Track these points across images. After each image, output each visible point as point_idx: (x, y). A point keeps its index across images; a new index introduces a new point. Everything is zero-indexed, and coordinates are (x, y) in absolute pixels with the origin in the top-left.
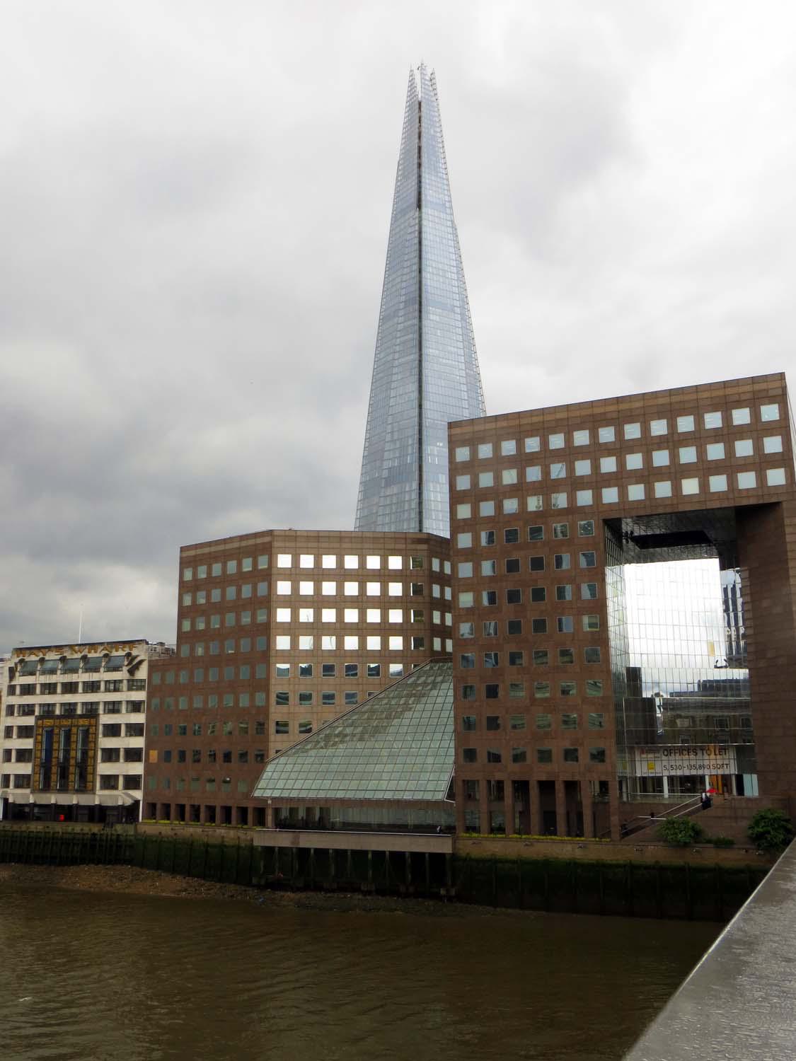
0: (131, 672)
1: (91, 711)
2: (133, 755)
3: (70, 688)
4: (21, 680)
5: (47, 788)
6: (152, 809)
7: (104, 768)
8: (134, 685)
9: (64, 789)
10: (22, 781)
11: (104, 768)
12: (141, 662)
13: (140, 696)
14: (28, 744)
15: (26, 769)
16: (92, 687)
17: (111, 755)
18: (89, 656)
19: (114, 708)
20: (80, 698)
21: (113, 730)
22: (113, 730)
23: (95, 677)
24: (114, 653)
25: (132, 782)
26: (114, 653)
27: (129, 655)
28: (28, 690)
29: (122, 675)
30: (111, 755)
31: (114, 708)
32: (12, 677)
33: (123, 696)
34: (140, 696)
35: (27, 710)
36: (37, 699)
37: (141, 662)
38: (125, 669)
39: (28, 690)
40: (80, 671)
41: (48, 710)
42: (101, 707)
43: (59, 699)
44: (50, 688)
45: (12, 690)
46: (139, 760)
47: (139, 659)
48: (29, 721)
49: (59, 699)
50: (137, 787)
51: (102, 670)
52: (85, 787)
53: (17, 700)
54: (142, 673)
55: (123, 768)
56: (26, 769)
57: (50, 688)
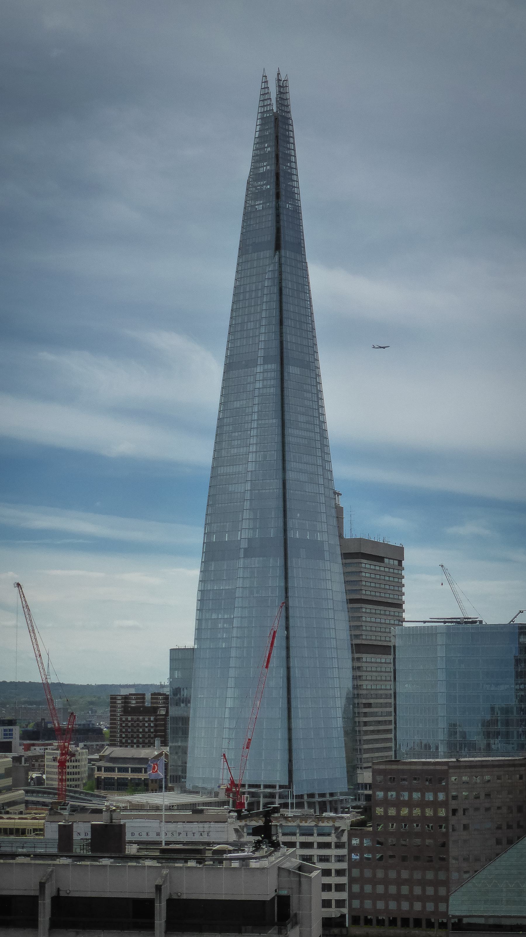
0: (338, 837)
6: (355, 920)
8: (339, 846)
12: (343, 831)
13: (344, 852)
18: (301, 824)
23: (309, 839)
24: (321, 824)
25: (340, 903)
26: (321, 824)
27: (334, 826)
32: (240, 836)
33: (332, 852)
34: (344, 852)
37: (343, 831)
38: (333, 835)
40: (298, 835)
42: (315, 859)
46: (344, 890)
47: (341, 829)
50: (344, 907)
51: (315, 835)
54: (345, 838)
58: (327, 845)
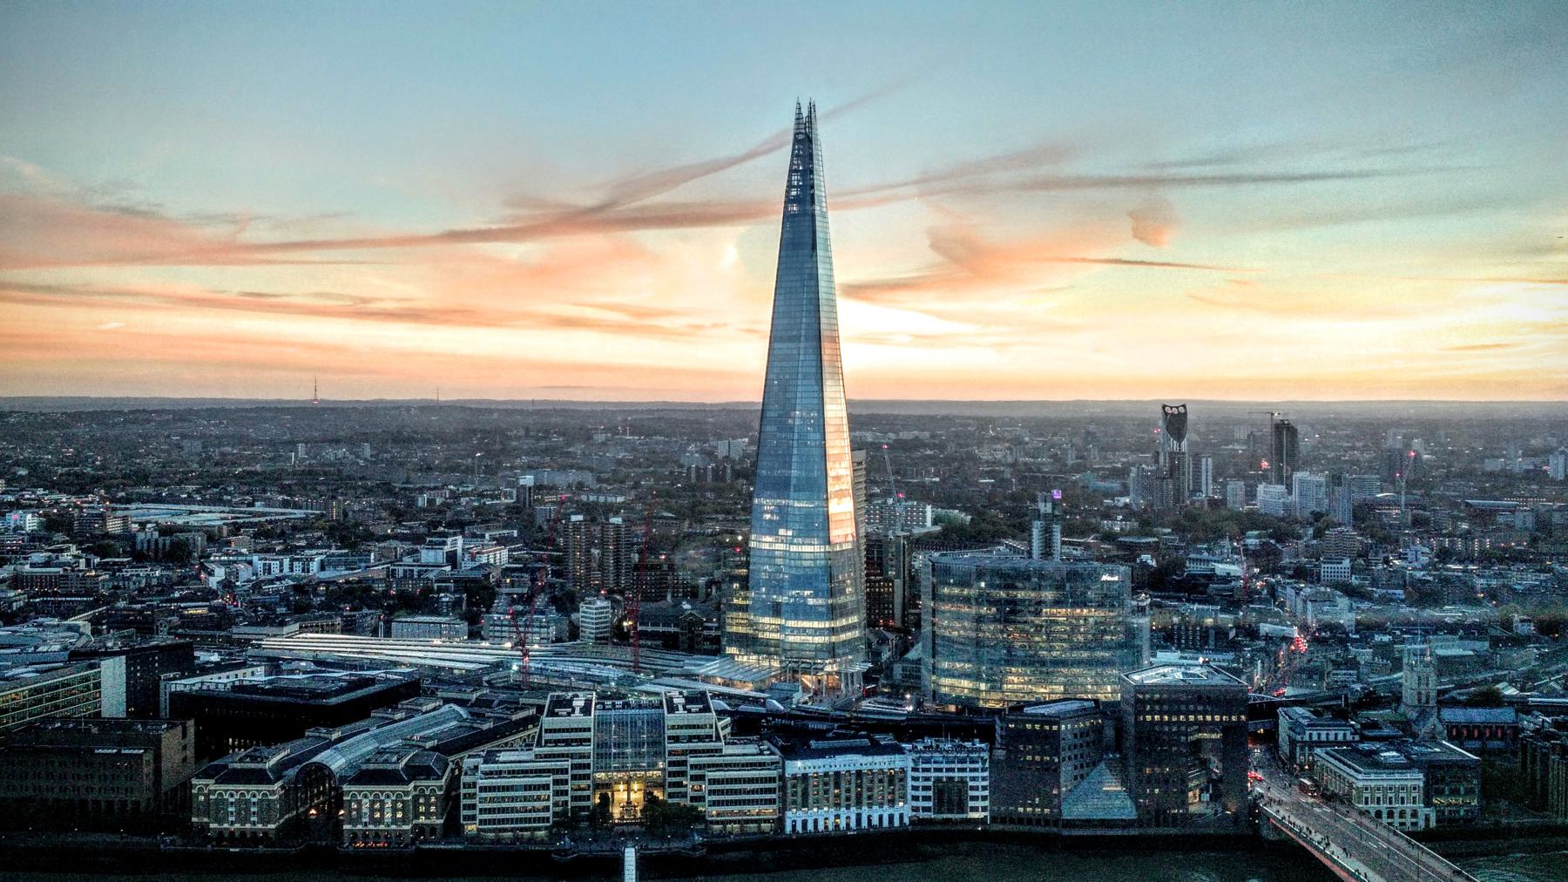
1: (963, 781)
2: (984, 798)
3: (952, 770)
4: (921, 766)
5: (940, 812)
6: (994, 819)
7: (971, 804)
8: (983, 770)
9: (950, 811)
10: (926, 809)
11: (971, 804)
14: (930, 793)
15: (930, 804)
16: (964, 770)
17: (974, 798)
19: (973, 779)
20: (956, 775)
21: (977, 788)
22: (977, 788)
25: (984, 809)
28: (925, 770)
29: (979, 765)
30: (974, 798)
31: (973, 779)
35: (927, 779)
36: (933, 774)
39: (925, 770)
41: (938, 780)
43: (944, 774)
44: (940, 770)
45: (914, 770)
48: (930, 783)
49: (944, 774)
52: (962, 810)
53: (920, 774)
55: (980, 804)
56: (930, 804)
57: (940, 770)
58: (975, 770)
